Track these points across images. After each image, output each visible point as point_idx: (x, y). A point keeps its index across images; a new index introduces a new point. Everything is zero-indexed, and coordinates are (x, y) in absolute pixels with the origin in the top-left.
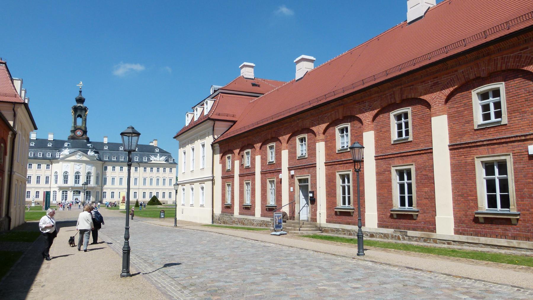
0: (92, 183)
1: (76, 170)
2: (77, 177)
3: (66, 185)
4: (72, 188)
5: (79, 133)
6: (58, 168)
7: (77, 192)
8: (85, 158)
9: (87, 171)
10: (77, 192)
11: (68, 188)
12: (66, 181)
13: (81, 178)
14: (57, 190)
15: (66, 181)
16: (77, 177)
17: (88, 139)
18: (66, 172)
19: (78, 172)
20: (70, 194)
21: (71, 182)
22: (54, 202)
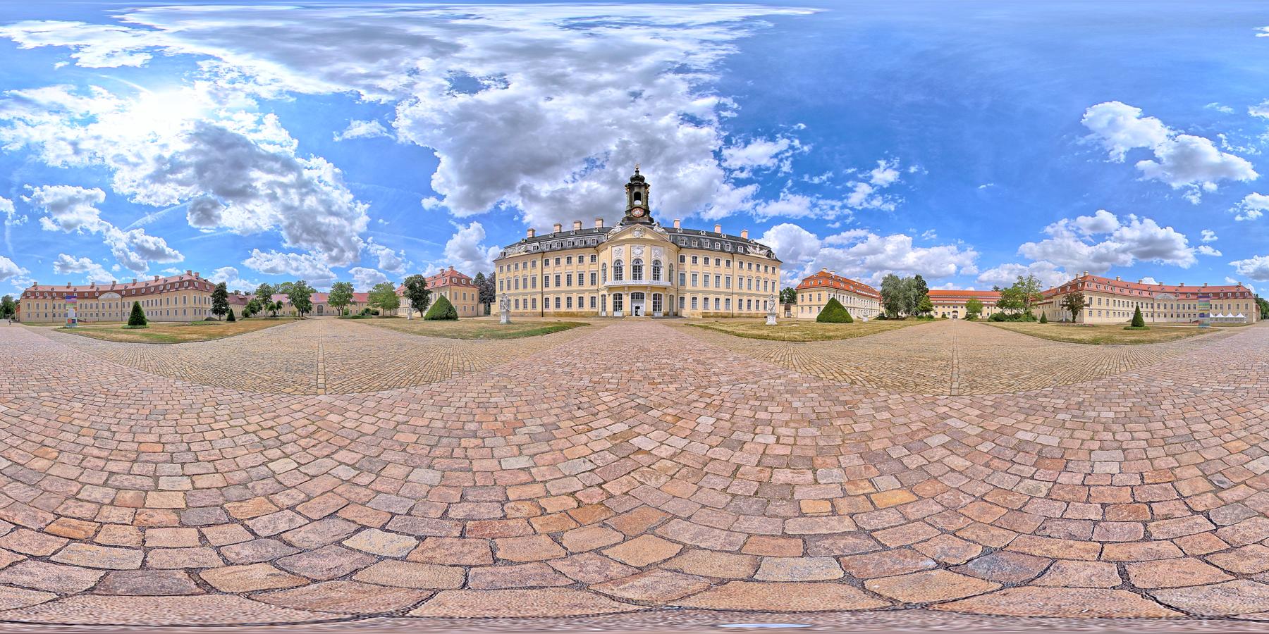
0: (663, 281)
1: (634, 257)
2: (637, 269)
3: (619, 283)
4: (630, 287)
5: (637, 212)
6: (607, 256)
7: (637, 297)
8: (648, 236)
9: (653, 258)
10: (637, 297)
11: (623, 288)
12: (618, 276)
13: (644, 269)
14: (605, 292)
15: (618, 276)
16: (637, 269)
17: (652, 220)
18: (618, 261)
19: (638, 260)
20: (627, 300)
21: (627, 279)
22: (604, 314)
